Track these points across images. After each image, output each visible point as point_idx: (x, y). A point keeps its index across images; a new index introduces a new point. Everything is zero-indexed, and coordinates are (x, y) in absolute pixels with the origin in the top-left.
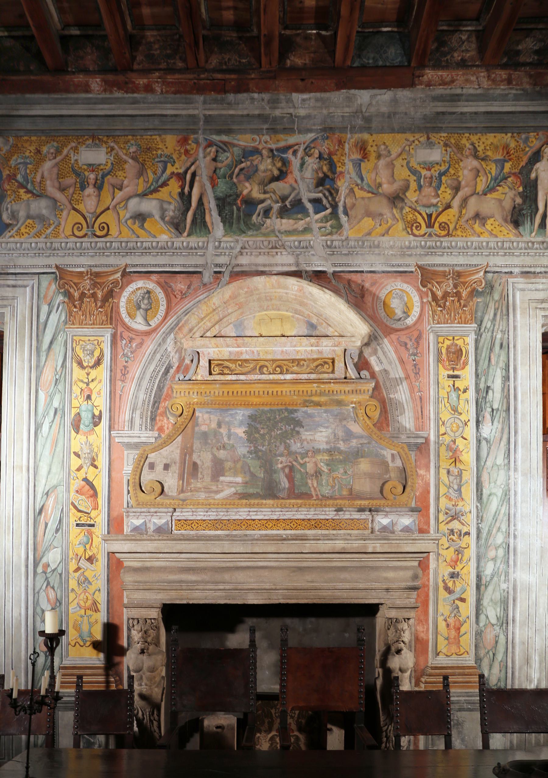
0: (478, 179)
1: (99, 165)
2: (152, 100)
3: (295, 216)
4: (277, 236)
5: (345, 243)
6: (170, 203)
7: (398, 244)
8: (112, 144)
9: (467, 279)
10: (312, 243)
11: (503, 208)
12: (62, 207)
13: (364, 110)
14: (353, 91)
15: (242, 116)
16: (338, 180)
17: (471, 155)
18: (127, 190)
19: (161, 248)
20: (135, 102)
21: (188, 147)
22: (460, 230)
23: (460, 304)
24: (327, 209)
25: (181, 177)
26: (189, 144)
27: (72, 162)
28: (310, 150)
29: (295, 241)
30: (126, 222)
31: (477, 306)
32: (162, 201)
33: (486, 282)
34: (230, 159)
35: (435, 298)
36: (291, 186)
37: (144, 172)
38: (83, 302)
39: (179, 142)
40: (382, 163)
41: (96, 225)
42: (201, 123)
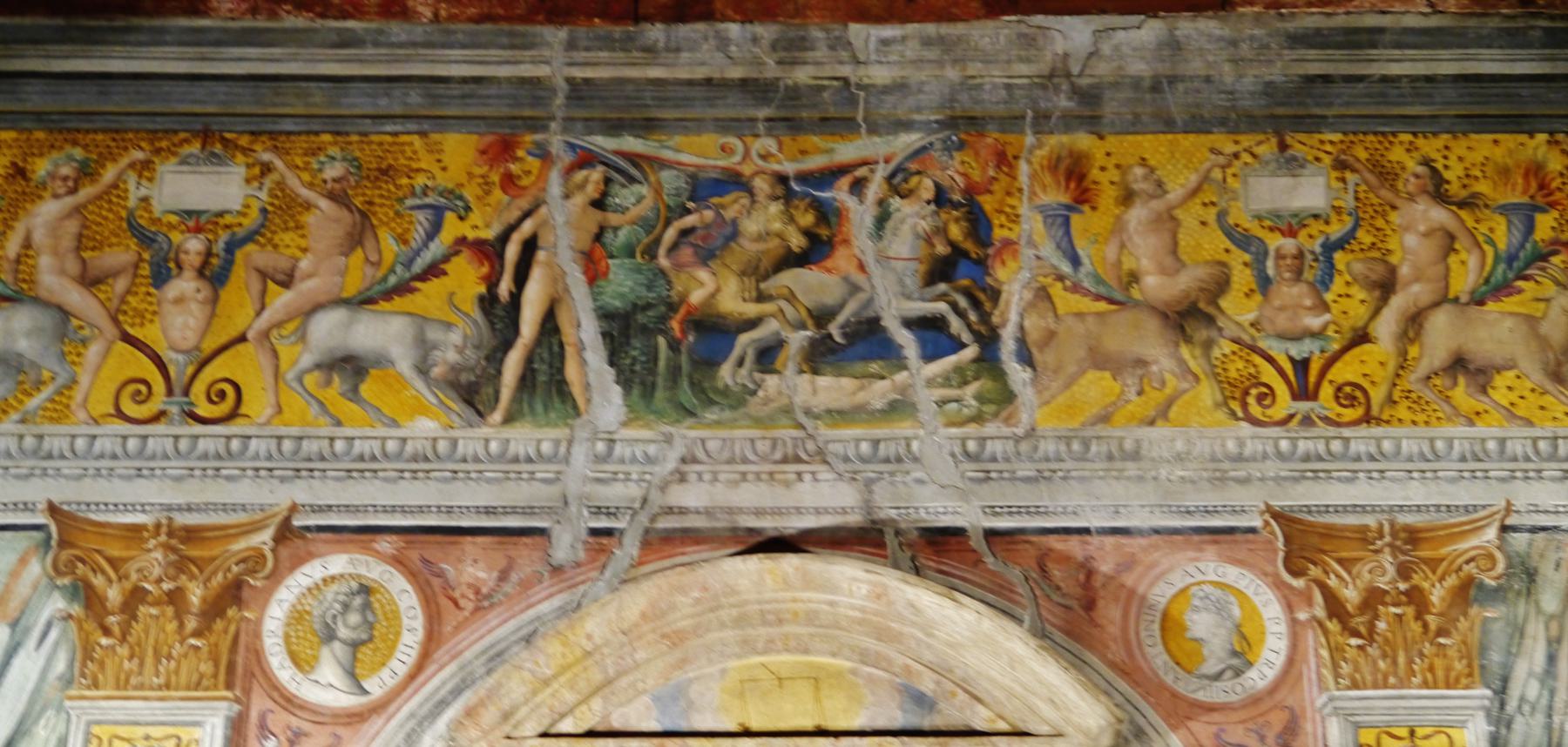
0: (1453, 260)
1: (221, 214)
2: (403, 37)
3: (859, 367)
4: (801, 427)
5: (1024, 447)
6: (449, 326)
7: (1202, 447)
8: (266, 157)
9: (1444, 551)
10: (915, 446)
11: (1543, 342)
12: (86, 332)
13: (1075, 70)
14: (1039, 19)
15: (690, 83)
16: (998, 265)
17: (1426, 192)
19: (415, 458)
20: (346, 41)
21: (514, 168)
22: (1406, 403)
23: (1425, 626)
24: (963, 346)
25: (489, 252)
26: (520, 159)
27: (132, 203)
28: (906, 180)
29: (858, 441)
30: (300, 380)
31: (1485, 632)
32: (421, 320)
33: (1508, 557)
34: (648, 202)
35: (1335, 606)
36: (846, 279)
37: (369, 234)
38: (134, 617)
39: (483, 152)
40: (1137, 215)
41: (199, 388)
42: (560, 100)
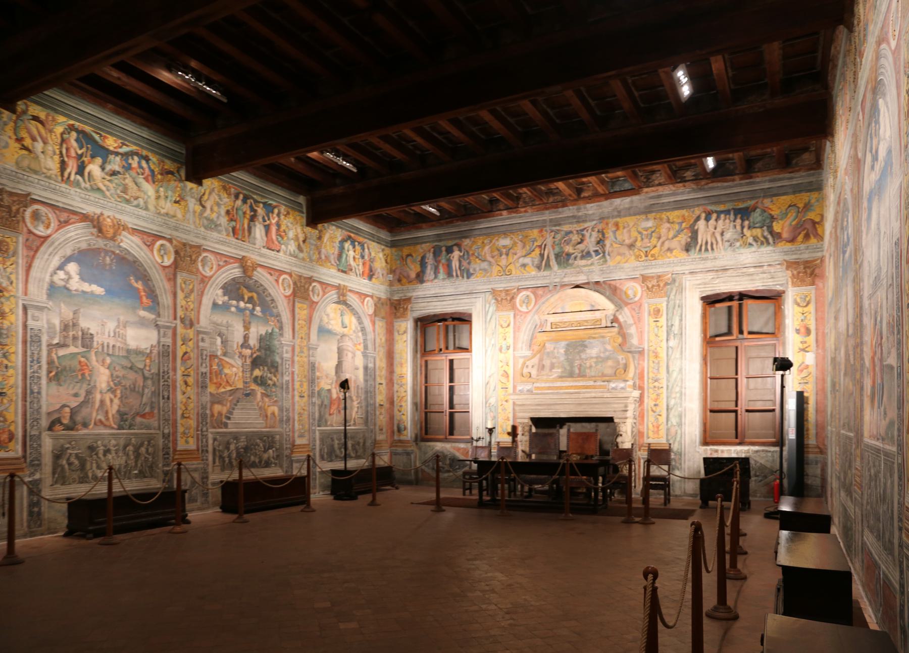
18: (519, 255)
20: (521, 217)
25: (540, 247)
35: (648, 288)
40: (625, 230)
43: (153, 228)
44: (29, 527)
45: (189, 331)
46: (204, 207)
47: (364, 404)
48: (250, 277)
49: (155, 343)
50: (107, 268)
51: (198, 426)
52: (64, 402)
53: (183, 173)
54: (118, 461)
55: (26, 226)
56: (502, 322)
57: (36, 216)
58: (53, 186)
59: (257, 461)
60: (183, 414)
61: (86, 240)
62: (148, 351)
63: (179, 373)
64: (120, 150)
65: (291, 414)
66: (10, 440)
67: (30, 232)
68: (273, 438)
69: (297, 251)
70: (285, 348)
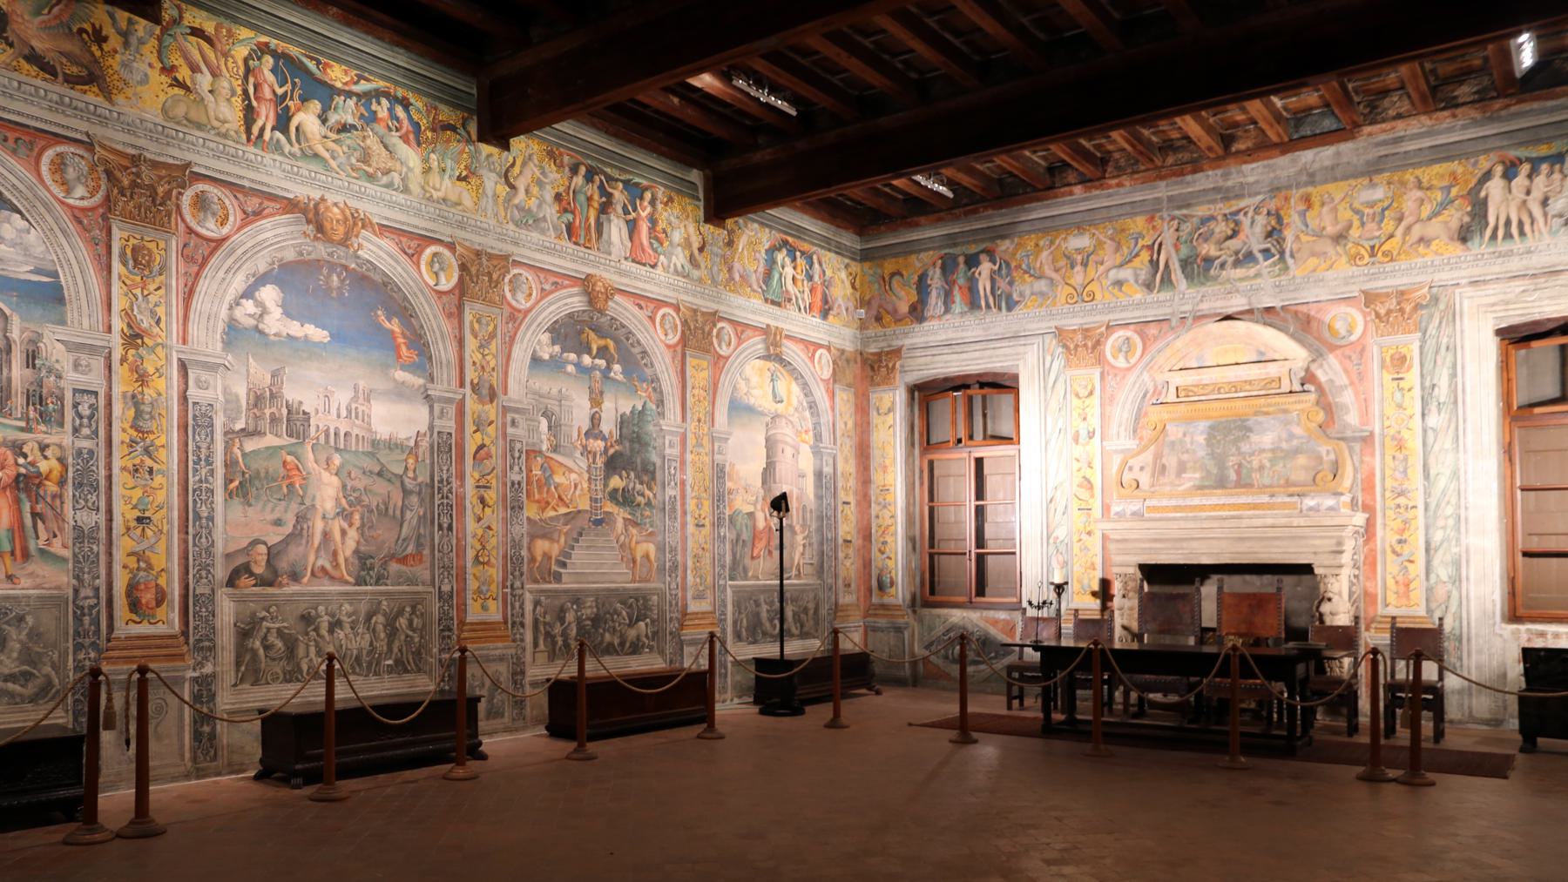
20: (1110, 196)
35: (1378, 315)
40: (1325, 209)
43: (419, 224)
44: (194, 759)
45: (488, 407)
46: (512, 187)
47: (815, 540)
48: (602, 312)
49: (424, 428)
50: (334, 294)
51: (505, 579)
52: (256, 535)
53: (473, 128)
54: (352, 641)
55: (183, 220)
56: (1078, 389)
57: (201, 203)
58: (232, 151)
59: (616, 642)
60: (477, 557)
61: (294, 246)
62: (412, 443)
63: (470, 483)
64: (355, 88)
65: (679, 558)
66: (159, 603)
67: (190, 231)
68: (646, 600)
69: (688, 266)
70: (668, 438)
